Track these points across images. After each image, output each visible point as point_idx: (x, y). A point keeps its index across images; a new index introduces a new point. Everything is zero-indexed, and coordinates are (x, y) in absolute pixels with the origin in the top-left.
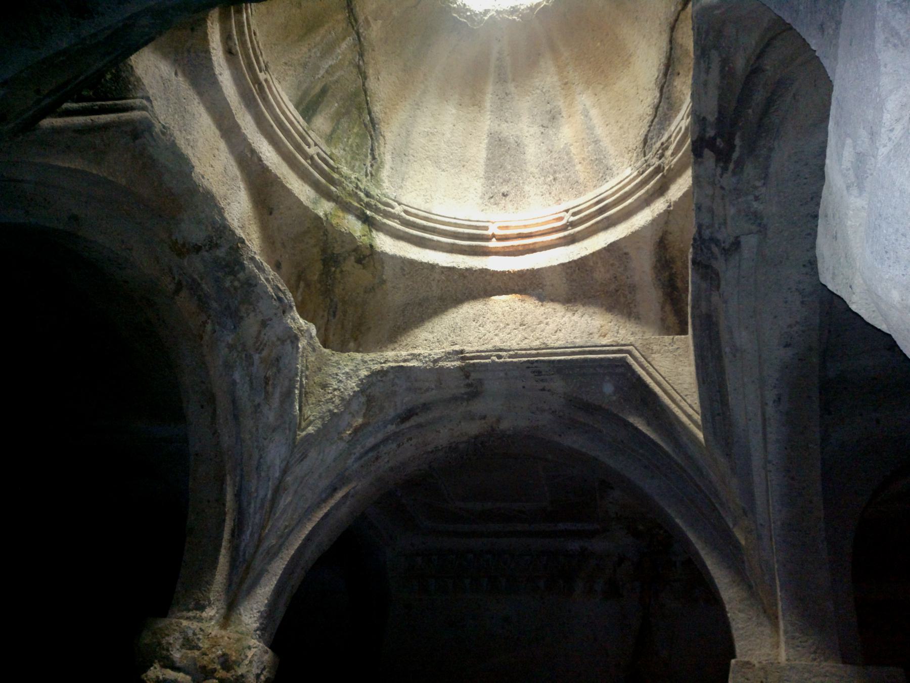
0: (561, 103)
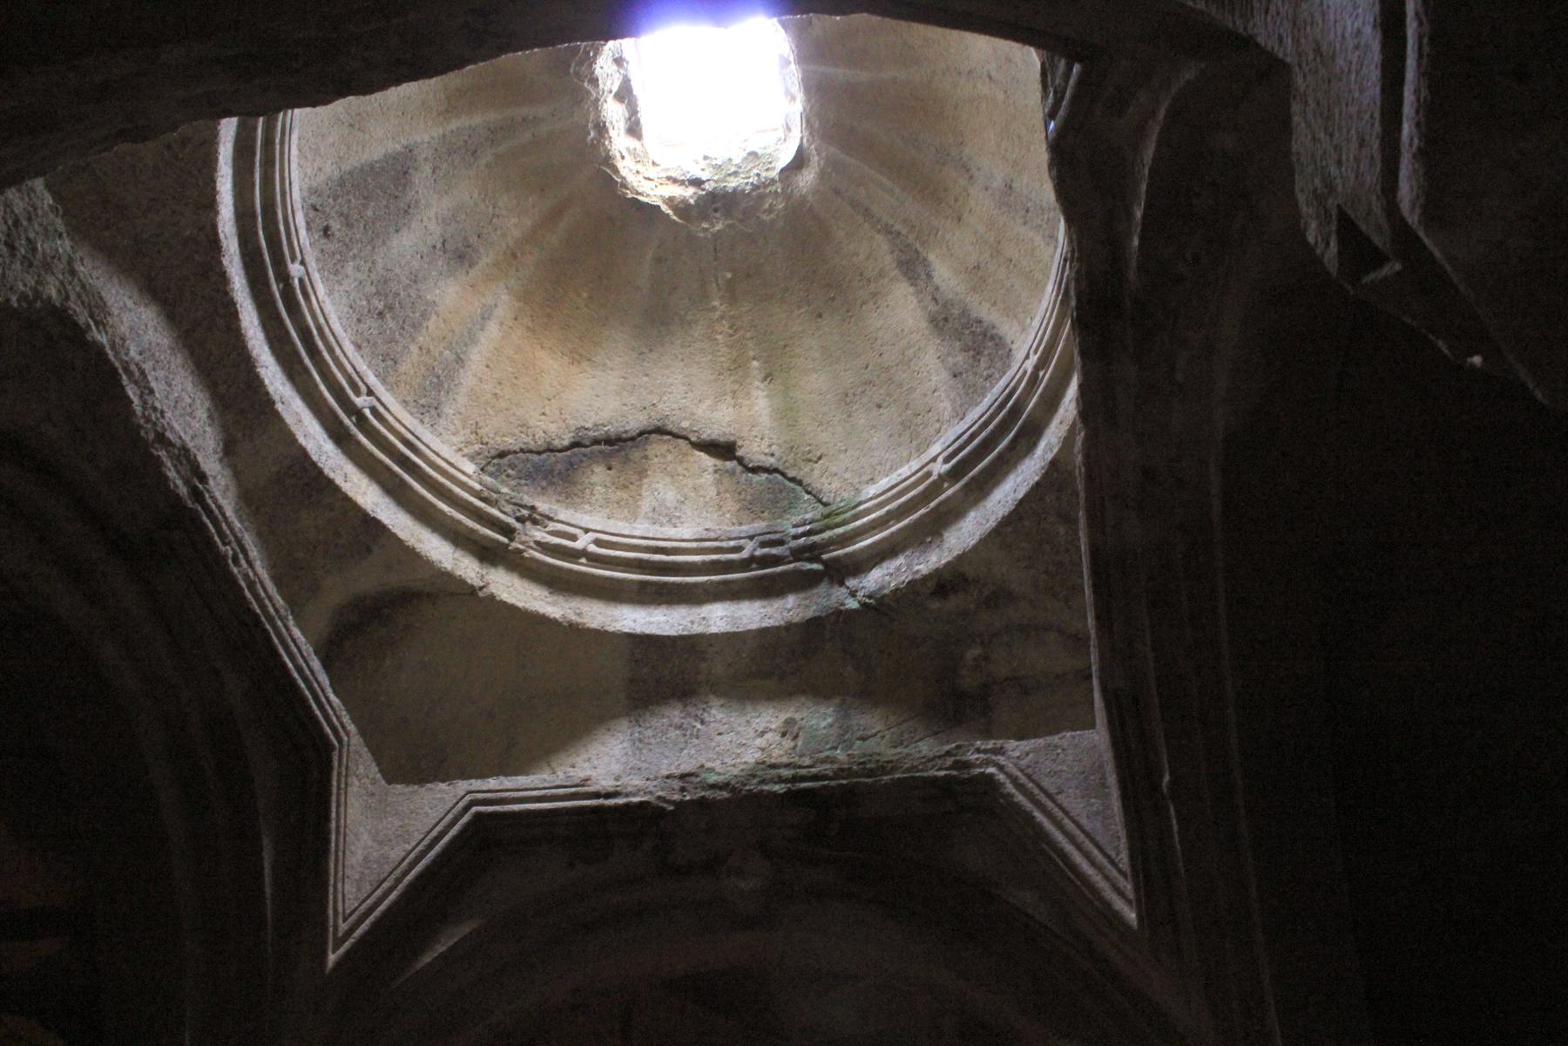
0: (486, 260)
